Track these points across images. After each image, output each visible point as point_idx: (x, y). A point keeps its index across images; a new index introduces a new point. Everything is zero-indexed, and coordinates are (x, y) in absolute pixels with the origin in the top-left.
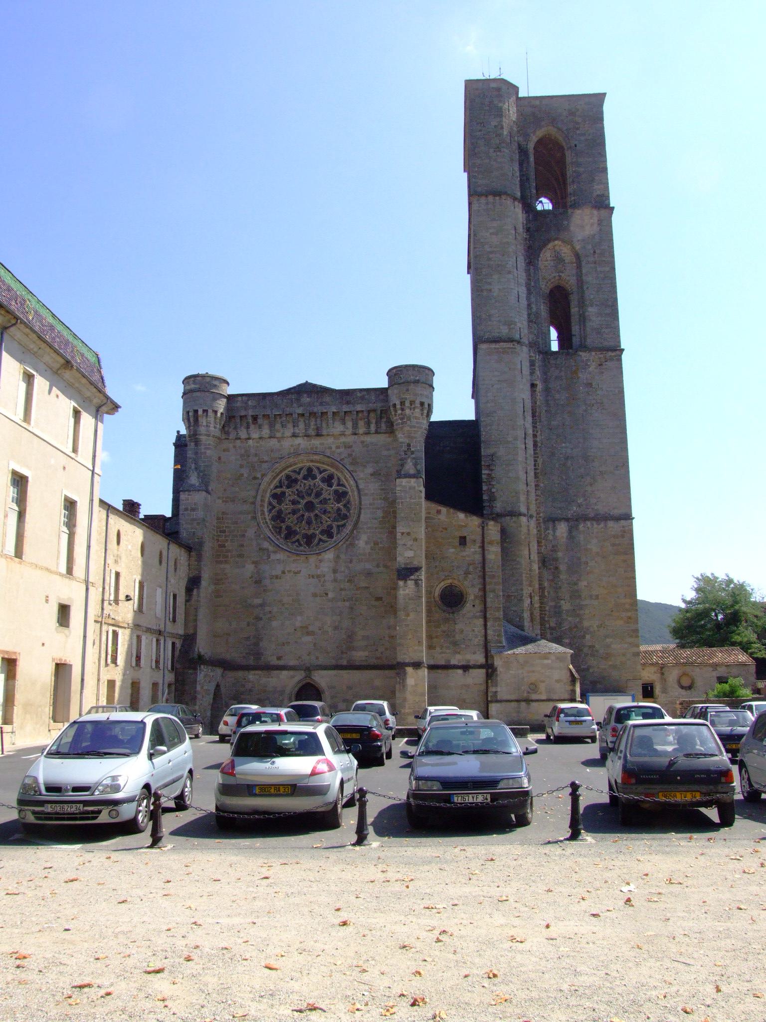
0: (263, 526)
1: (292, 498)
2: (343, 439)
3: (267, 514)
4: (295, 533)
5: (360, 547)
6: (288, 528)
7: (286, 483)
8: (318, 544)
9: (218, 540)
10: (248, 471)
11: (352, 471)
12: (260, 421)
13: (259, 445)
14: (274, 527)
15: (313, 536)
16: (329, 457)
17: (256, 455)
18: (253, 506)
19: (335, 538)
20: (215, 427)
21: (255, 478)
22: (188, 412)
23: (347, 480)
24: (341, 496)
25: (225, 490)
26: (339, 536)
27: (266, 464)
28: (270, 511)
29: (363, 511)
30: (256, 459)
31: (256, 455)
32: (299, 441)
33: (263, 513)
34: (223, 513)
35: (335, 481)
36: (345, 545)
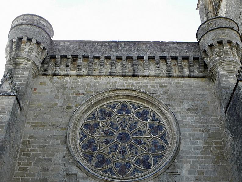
0: (73, 151)
1: (105, 129)
2: (157, 80)
3: (78, 141)
4: (107, 161)
5: (182, 177)
6: (100, 156)
7: (100, 115)
8: (133, 174)
9: (19, 163)
10: (62, 102)
11: (169, 105)
12: (79, 61)
13: (76, 81)
14: (83, 154)
15: (128, 165)
16: (145, 93)
17: (72, 88)
18: (65, 131)
19: (152, 168)
20: (37, 57)
21: (69, 107)
22: (12, 41)
23: (163, 114)
24: (156, 128)
25: (36, 116)
26: (157, 166)
27: (81, 96)
28: (81, 139)
29: (182, 141)
30: (72, 92)
31: (72, 88)
32: (116, 79)
33: (74, 139)
34: (31, 137)
35: (150, 116)
36: (165, 174)
